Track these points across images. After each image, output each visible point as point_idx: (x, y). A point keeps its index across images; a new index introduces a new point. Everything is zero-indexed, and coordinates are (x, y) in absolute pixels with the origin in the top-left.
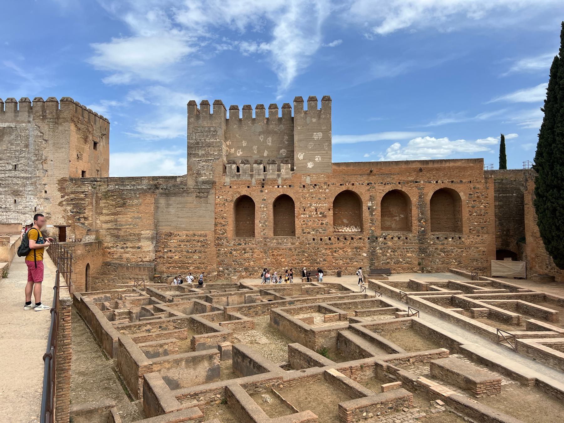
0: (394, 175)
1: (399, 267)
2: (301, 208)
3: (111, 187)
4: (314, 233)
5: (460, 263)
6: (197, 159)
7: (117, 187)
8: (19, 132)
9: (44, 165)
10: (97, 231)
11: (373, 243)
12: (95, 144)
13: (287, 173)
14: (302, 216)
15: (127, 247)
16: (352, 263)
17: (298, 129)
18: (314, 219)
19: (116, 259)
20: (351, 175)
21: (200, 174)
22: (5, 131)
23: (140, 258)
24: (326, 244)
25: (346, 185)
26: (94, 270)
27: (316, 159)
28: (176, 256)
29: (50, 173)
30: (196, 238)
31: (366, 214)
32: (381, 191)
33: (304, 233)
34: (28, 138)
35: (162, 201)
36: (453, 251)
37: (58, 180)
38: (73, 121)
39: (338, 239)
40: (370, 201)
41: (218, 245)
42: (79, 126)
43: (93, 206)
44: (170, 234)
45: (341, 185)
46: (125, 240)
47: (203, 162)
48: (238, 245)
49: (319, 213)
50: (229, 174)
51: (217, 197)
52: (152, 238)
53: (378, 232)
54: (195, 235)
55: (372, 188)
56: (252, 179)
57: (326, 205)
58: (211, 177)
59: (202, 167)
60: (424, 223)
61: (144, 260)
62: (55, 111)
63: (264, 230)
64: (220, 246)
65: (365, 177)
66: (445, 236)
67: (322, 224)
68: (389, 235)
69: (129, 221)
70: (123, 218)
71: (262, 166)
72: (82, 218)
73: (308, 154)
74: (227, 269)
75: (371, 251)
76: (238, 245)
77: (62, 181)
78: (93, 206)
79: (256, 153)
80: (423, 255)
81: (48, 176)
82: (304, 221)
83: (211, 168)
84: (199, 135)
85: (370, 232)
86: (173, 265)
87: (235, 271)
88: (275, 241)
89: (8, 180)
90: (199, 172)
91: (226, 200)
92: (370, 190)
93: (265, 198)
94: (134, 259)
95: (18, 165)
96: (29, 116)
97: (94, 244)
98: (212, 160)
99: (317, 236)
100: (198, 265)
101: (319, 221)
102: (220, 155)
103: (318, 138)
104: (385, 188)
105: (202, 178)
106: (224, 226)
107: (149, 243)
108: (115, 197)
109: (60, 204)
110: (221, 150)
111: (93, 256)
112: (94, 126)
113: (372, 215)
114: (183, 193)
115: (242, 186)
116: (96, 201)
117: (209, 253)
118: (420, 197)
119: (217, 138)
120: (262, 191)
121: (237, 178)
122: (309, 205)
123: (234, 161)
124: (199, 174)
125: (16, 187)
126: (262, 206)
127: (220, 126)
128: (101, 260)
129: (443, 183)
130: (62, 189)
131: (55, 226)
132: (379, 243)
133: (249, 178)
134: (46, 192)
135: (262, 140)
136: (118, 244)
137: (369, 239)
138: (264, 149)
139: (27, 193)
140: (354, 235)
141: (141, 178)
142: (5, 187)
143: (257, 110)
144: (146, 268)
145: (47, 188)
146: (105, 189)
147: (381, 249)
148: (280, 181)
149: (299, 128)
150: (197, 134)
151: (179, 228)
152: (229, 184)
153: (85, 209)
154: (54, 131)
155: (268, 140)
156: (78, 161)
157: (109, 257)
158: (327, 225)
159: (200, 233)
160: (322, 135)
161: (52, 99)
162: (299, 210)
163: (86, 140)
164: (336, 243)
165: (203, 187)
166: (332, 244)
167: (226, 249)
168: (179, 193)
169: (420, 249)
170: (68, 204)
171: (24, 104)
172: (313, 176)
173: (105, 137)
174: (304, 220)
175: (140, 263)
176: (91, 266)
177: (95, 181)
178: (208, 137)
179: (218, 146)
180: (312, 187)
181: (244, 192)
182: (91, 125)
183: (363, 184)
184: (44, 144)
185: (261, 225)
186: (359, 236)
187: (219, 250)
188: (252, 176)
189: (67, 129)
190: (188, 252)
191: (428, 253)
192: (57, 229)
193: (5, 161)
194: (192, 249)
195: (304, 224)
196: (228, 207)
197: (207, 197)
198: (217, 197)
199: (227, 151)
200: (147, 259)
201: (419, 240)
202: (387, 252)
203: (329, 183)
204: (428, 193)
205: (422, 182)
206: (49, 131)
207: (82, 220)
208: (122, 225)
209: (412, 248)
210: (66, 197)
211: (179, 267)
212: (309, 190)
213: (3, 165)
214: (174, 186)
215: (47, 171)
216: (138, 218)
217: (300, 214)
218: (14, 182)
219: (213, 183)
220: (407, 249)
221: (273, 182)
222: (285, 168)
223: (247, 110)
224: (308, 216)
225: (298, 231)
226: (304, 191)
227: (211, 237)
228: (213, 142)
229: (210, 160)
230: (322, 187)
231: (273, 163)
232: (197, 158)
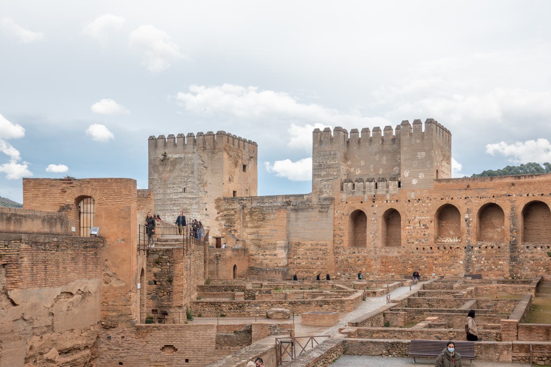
0: (488, 189)
1: (491, 274)
2: (406, 221)
3: (254, 204)
4: (417, 243)
5: (548, 270)
6: (320, 179)
7: (258, 204)
8: (187, 161)
9: (205, 188)
10: (244, 241)
11: (469, 252)
12: (244, 167)
13: (395, 190)
14: (407, 228)
15: (266, 255)
16: (450, 270)
17: (405, 150)
18: (417, 231)
19: (258, 264)
20: (451, 190)
21: (322, 192)
22: (177, 161)
23: (276, 263)
24: (428, 253)
25: (446, 199)
26: (241, 272)
27: (419, 176)
28: (303, 262)
29: (209, 194)
30: (319, 247)
31: (463, 224)
32: (477, 204)
33: (409, 243)
34: (193, 166)
35: (293, 215)
36: (542, 259)
37: (215, 200)
38: (226, 150)
39: (438, 248)
40: (467, 214)
41: (337, 253)
42: (231, 153)
43: (240, 220)
44: (299, 244)
45: (442, 199)
46: (265, 249)
47: (324, 181)
48: (353, 253)
49: (422, 225)
50: (346, 191)
51: (336, 212)
52: (285, 247)
53: (473, 242)
54: (318, 244)
55: (469, 202)
56: (364, 195)
57: (428, 217)
58: (331, 194)
59: (324, 186)
60: (515, 234)
61: (279, 265)
62: (212, 143)
63: (374, 240)
64: (338, 254)
65: (463, 192)
66: (534, 246)
67: (424, 235)
68: (483, 244)
69: (268, 233)
70: (263, 230)
71: (373, 184)
72: (233, 230)
73: (413, 171)
74: (344, 274)
75: (467, 259)
76: (353, 253)
77: (218, 200)
78: (240, 220)
79: (372, 171)
80: (514, 263)
81: (207, 197)
82: (409, 232)
83: (331, 186)
84: (322, 159)
85: (467, 242)
86: (301, 270)
87: (350, 275)
88: (383, 250)
89: (180, 201)
90: (322, 190)
91: (343, 214)
92: (468, 203)
93: (375, 212)
94: (271, 265)
95: (186, 188)
96: (194, 148)
97: (240, 251)
98: (332, 179)
99: (420, 246)
100: (320, 270)
101: (422, 232)
102: (338, 175)
103: (422, 157)
104: (480, 202)
105: (324, 195)
106: (341, 236)
107: (283, 251)
108: (257, 213)
109: (217, 219)
110: (340, 170)
111: (239, 260)
112: (243, 151)
113: (468, 226)
114: (309, 208)
115: (356, 201)
116: (243, 217)
117: (328, 260)
118: (512, 209)
119: (336, 160)
120: (373, 206)
121: (352, 195)
122: (413, 218)
123: (350, 180)
124: (321, 192)
125: (185, 206)
126: (373, 219)
127: (339, 150)
128: (247, 265)
129: (533, 196)
130: (218, 207)
131: (213, 237)
132: (474, 252)
133: (362, 195)
134: (206, 209)
135: (377, 159)
136: (260, 252)
137: (465, 248)
138: (380, 167)
139: (192, 210)
140: (452, 244)
141: (276, 197)
142: (177, 206)
143: (374, 132)
144: (281, 272)
145: (207, 206)
146: (250, 206)
147: (476, 257)
148: (388, 197)
149: (405, 149)
150: (320, 157)
151: (305, 239)
152: (345, 200)
153: (235, 223)
154: (211, 160)
155: (383, 159)
156: (230, 183)
157: (253, 263)
158: (428, 235)
159: (321, 242)
160: (425, 154)
161: (210, 133)
162: (405, 222)
163: (236, 165)
164: (436, 252)
165: (324, 203)
166: (433, 253)
167: (343, 257)
168: (306, 209)
169: (511, 256)
170: (222, 220)
171: (190, 138)
172: (417, 192)
173: (254, 159)
174: (409, 231)
175: (276, 268)
176: (238, 268)
177: (242, 200)
178: (329, 160)
179: (337, 167)
180: (416, 201)
181: (358, 207)
182: (241, 151)
183: (461, 198)
184: (204, 171)
185: (371, 236)
186: (457, 245)
187: (337, 257)
188: (364, 192)
189: (221, 157)
190: (312, 259)
191: (519, 261)
192: (215, 240)
193: (178, 186)
194: (316, 256)
195: (409, 235)
196: (345, 221)
197: (327, 212)
198: (336, 212)
199: (348, 170)
200: (281, 265)
201: (511, 249)
202: (481, 260)
203: (431, 198)
204: (520, 205)
205: (514, 195)
206: (208, 159)
207: (233, 232)
208: (262, 236)
209: (503, 257)
210: (221, 213)
211: (306, 272)
212: (413, 204)
213: (176, 188)
214: (302, 202)
215: (207, 192)
216: (274, 230)
217: (405, 226)
218: (184, 202)
219: (332, 199)
220: (499, 257)
221: (383, 197)
222: (392, 185)
223: (365, 133)
224: (412, 228)
225: (404, 242)
226: (409, 205)
227: (330, 246)
228: (333, 164)
229: (331, 179)
230: (425, 201)
231: (383, 180)
232: (320, 178)
